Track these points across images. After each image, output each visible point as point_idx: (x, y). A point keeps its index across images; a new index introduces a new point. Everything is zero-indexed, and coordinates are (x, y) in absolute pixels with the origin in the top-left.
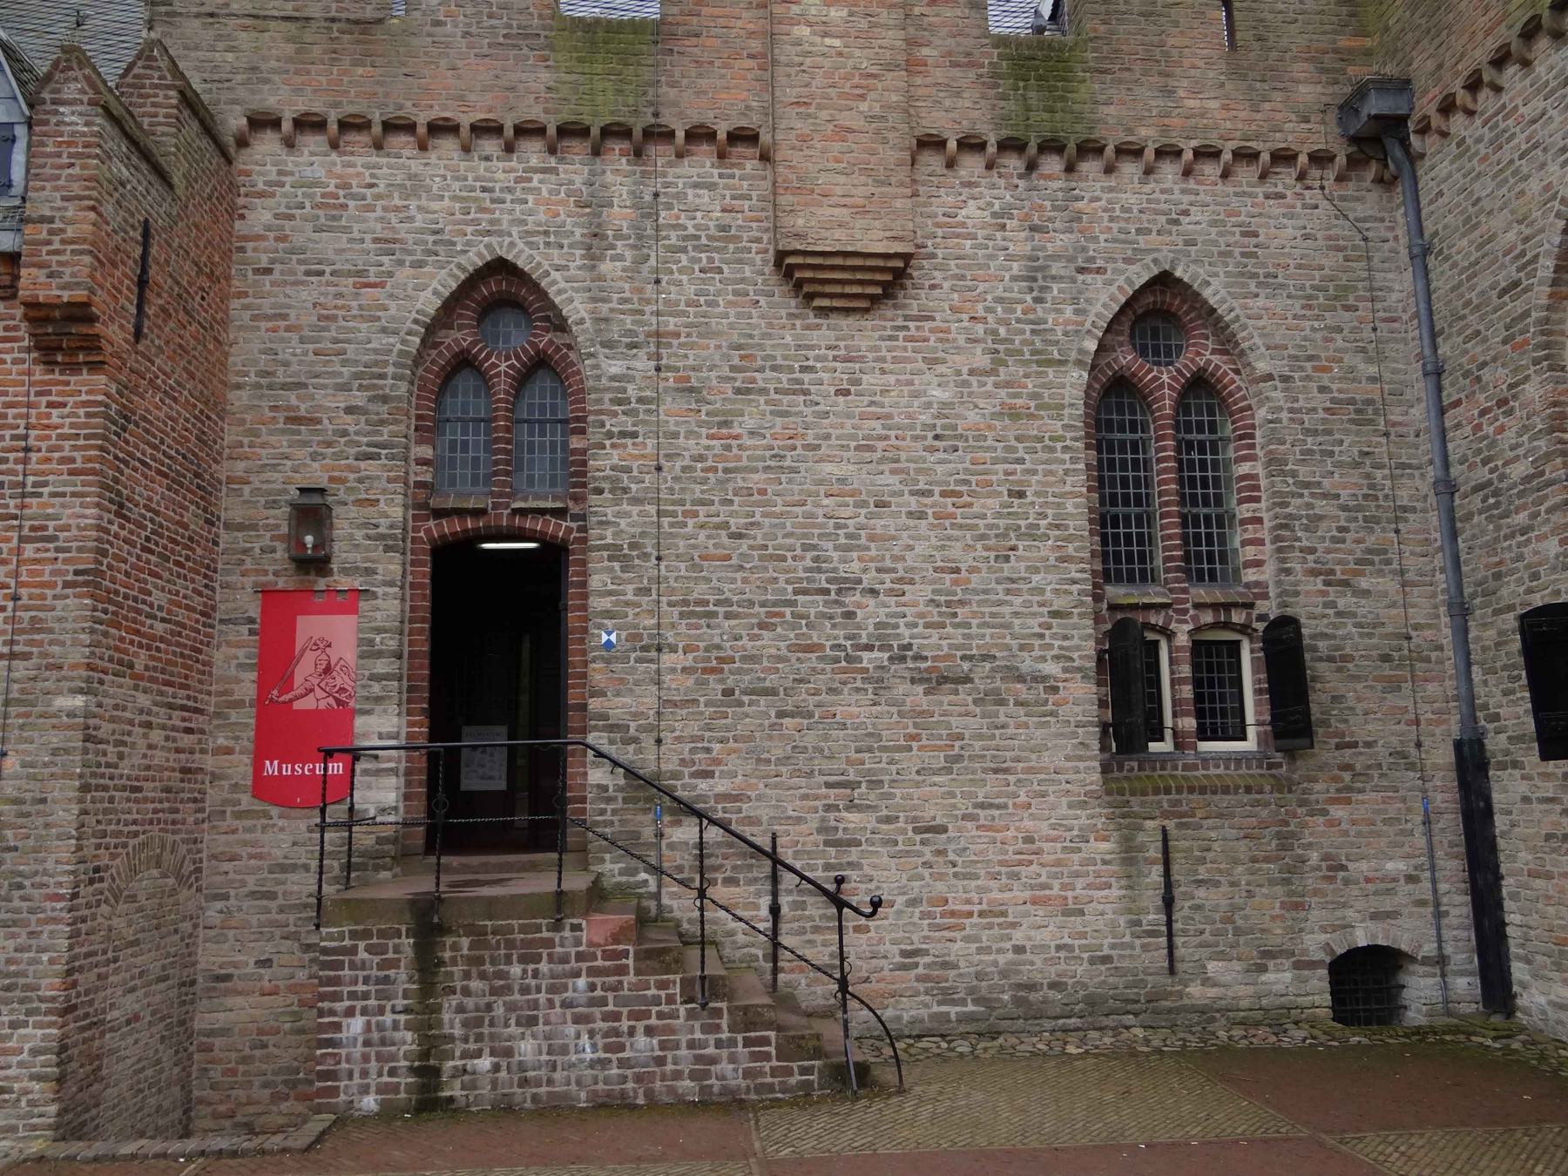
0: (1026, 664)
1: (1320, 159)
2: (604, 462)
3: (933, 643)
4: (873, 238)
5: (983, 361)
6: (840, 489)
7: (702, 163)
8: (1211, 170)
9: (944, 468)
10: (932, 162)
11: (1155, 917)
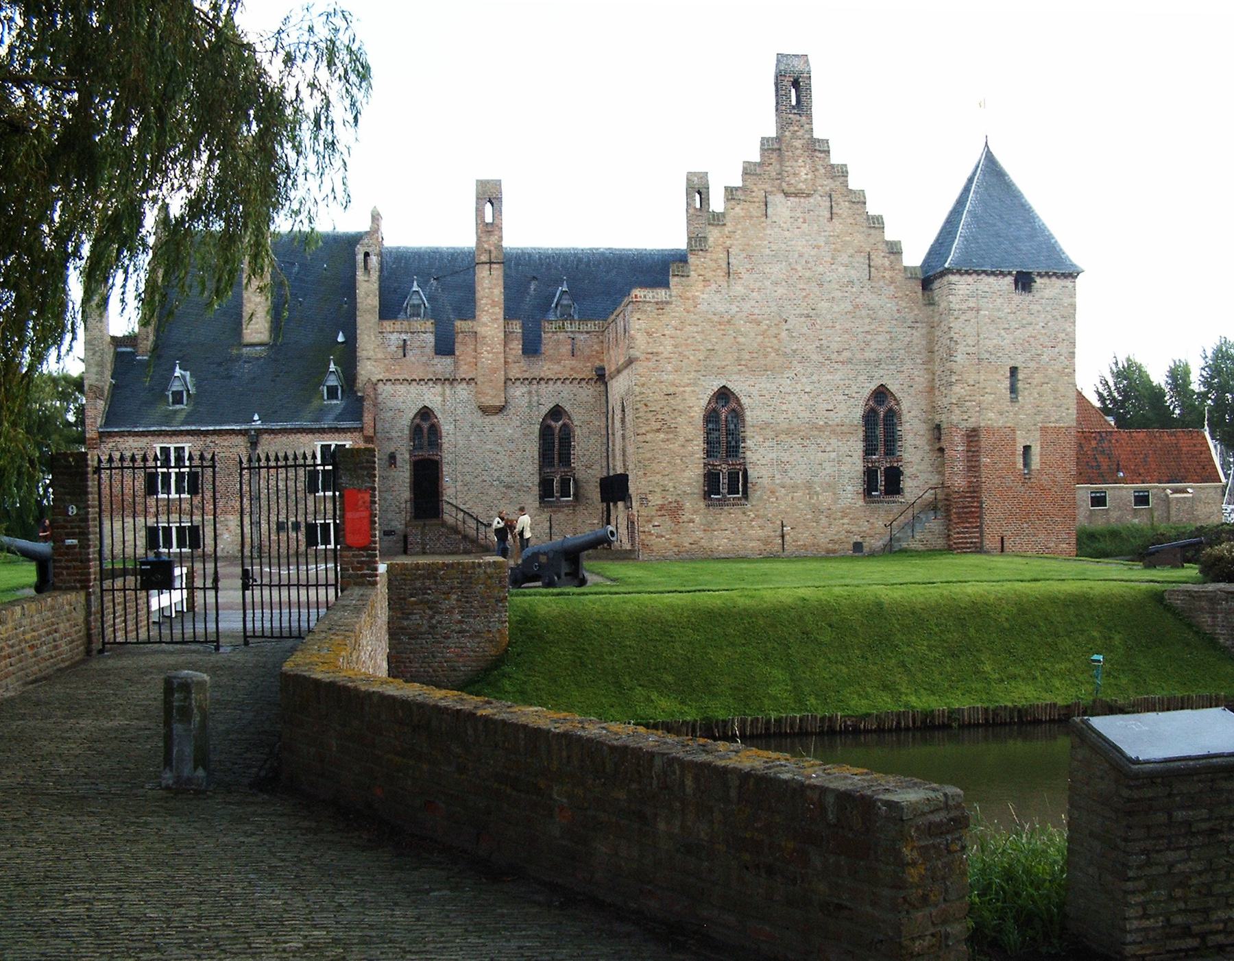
0: (525, 484)
1: (592, 379)
2: (445, 446)
3: (507, 480)
4: (498, 402)
5: (519, 424)
6: (490, 451)
7: (464, 385)
8: (568, 382)
9: (512, 446)
10: (509, 383)
11: (548, 531)
